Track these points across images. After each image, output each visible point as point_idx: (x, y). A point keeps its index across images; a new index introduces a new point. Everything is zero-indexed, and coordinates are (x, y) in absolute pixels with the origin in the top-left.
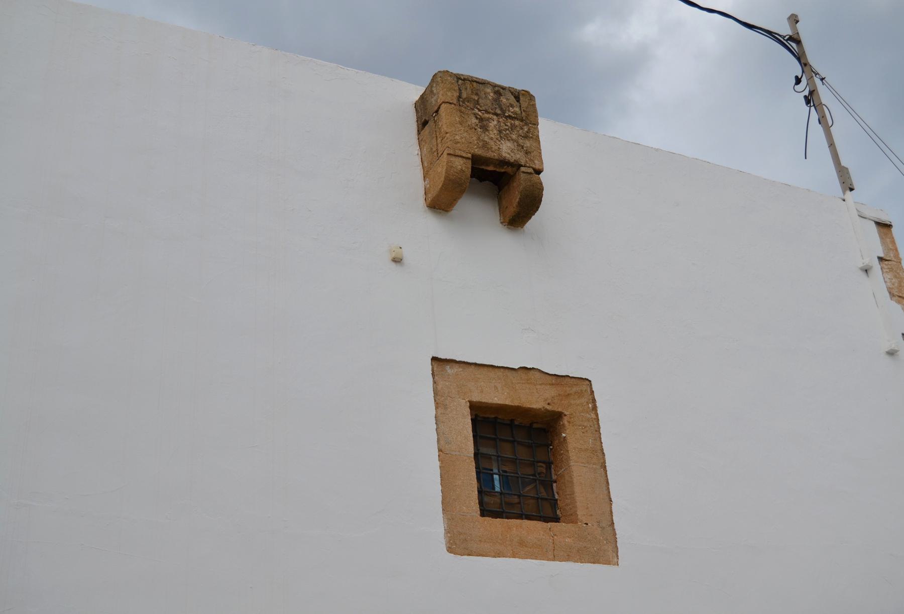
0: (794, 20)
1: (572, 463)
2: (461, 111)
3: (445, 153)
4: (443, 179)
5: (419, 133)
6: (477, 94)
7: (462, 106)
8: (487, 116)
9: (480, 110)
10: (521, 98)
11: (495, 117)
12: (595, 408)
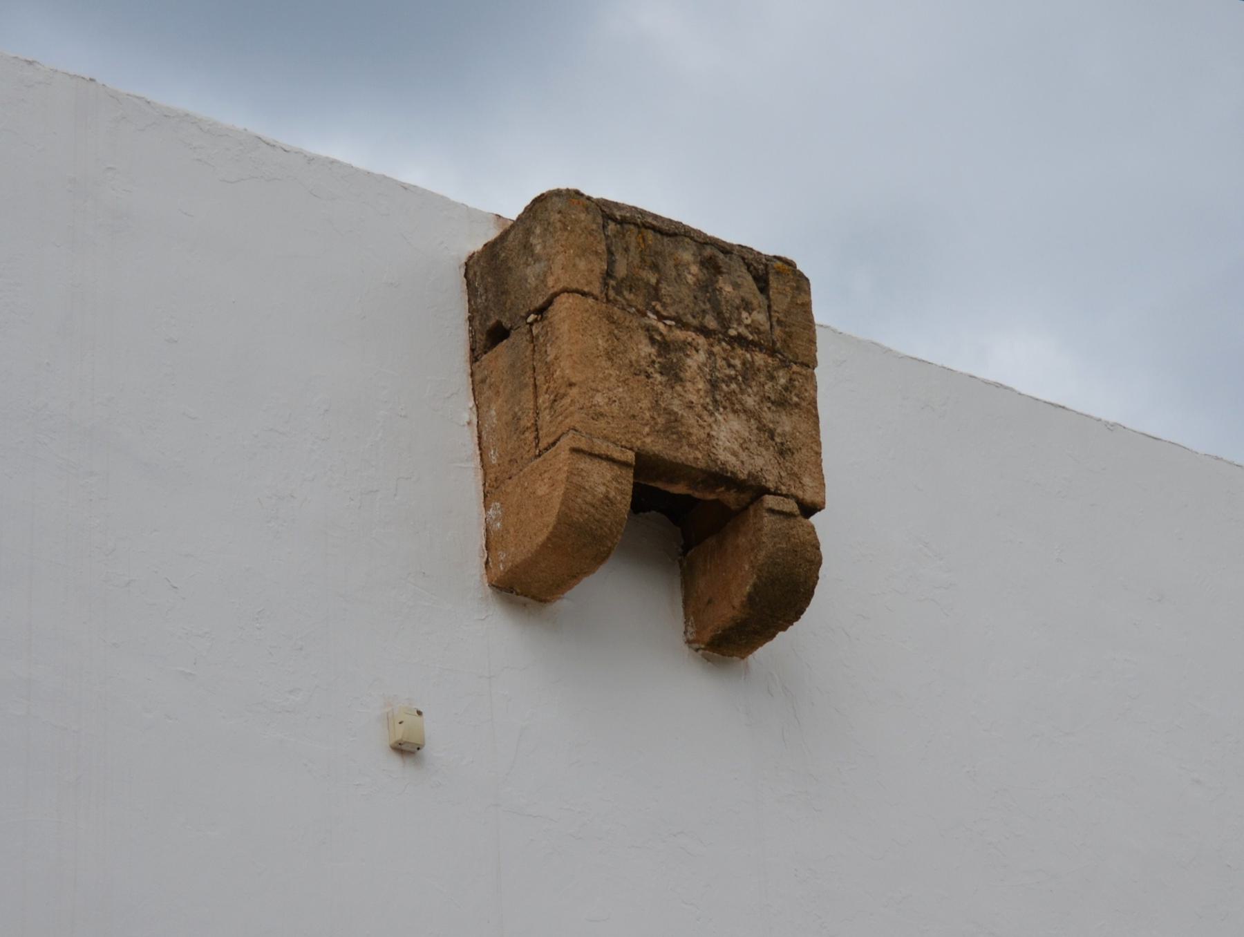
2: (610, 319)
3: (565, 443)
4: (551, 519)
5: (474, 358)
6: (655, 267)
7: (615, 302)
8: (680, 335)
9: (661, 318)
10: (773, 283)
11: (701, 340)
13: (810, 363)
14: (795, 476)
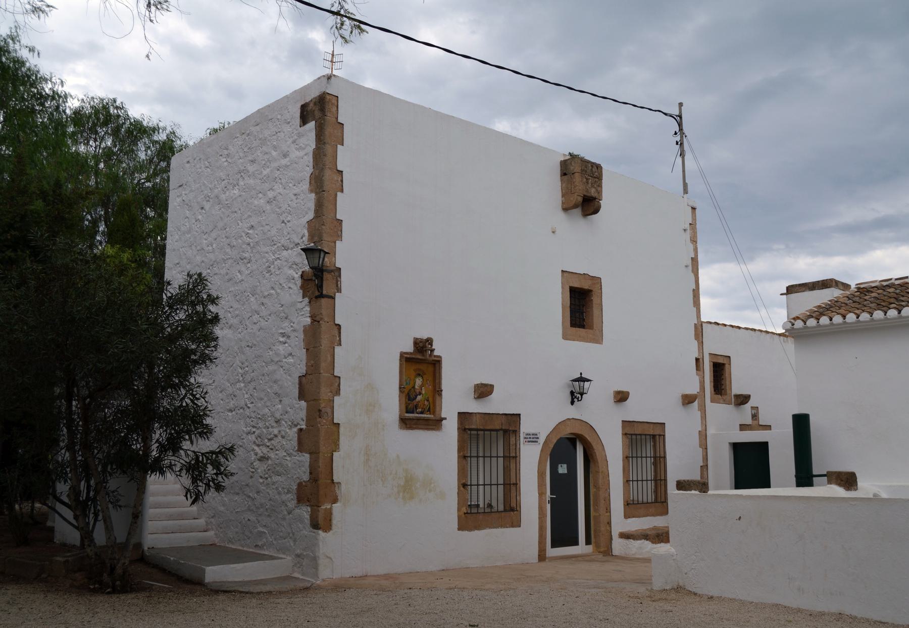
0: (681, 105)
1: (594, 309)
3: (576, 194)
5: (561, 176)
6: (586, 167)
12: (601, 288)
13: (602, 180)
14: (599, 196)
